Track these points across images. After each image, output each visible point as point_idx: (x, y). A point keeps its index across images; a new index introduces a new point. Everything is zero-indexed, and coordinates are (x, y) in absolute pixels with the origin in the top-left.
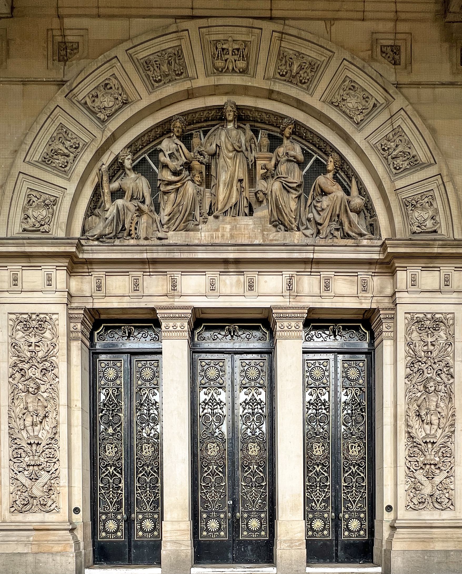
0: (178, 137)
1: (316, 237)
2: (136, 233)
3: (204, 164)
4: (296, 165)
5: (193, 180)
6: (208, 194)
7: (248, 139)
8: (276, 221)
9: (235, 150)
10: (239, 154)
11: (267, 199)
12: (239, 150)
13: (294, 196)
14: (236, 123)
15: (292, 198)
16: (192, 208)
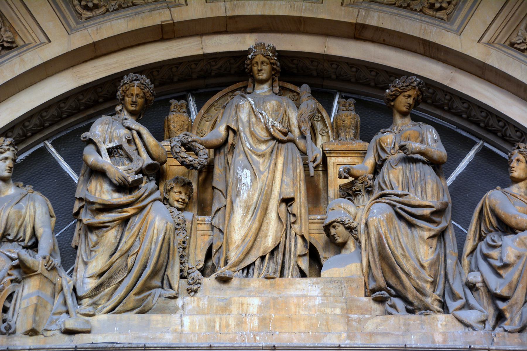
0: (132, 113)
1: (494, 328)
2: (4, 321)
3: (196, 168)
4: (428, 170)
5: (165, 198)
6: (204, 228)
7: (306, 116)
8: (380, 289)
9: (274, 138)
10: (284, 146)
11: (357, 239)
12: (285, 138)
13: (426, 234)
14: (276, 84)
15: (421, 238)
16: (161, 259)
